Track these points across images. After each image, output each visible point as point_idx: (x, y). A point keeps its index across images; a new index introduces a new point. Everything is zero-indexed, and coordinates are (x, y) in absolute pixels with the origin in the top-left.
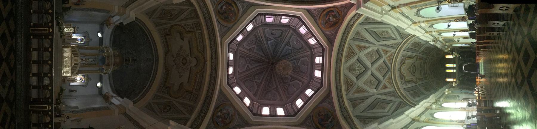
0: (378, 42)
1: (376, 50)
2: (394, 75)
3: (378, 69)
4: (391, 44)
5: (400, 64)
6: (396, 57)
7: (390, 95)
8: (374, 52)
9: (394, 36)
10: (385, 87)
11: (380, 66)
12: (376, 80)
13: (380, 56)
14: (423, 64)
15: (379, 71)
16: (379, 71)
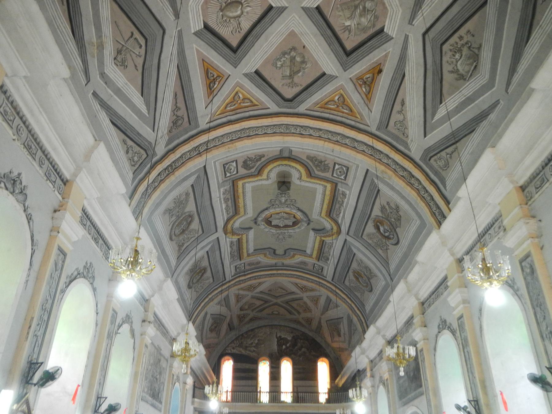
0: (424, 35)
1: (382, 30)
2: (265, 132)
3: (294, 49)
4: (403, 103)
5: (308, 157)
6: (339, 138)
7: (181, 104)
8: (377, 18)
9: (441, 112)
10: (214, 81)
11: (304, 57)
12: (244, 32)
13: (348, 54)
14: (299, 258)
15: (284, 54)
16: (284, 54)
